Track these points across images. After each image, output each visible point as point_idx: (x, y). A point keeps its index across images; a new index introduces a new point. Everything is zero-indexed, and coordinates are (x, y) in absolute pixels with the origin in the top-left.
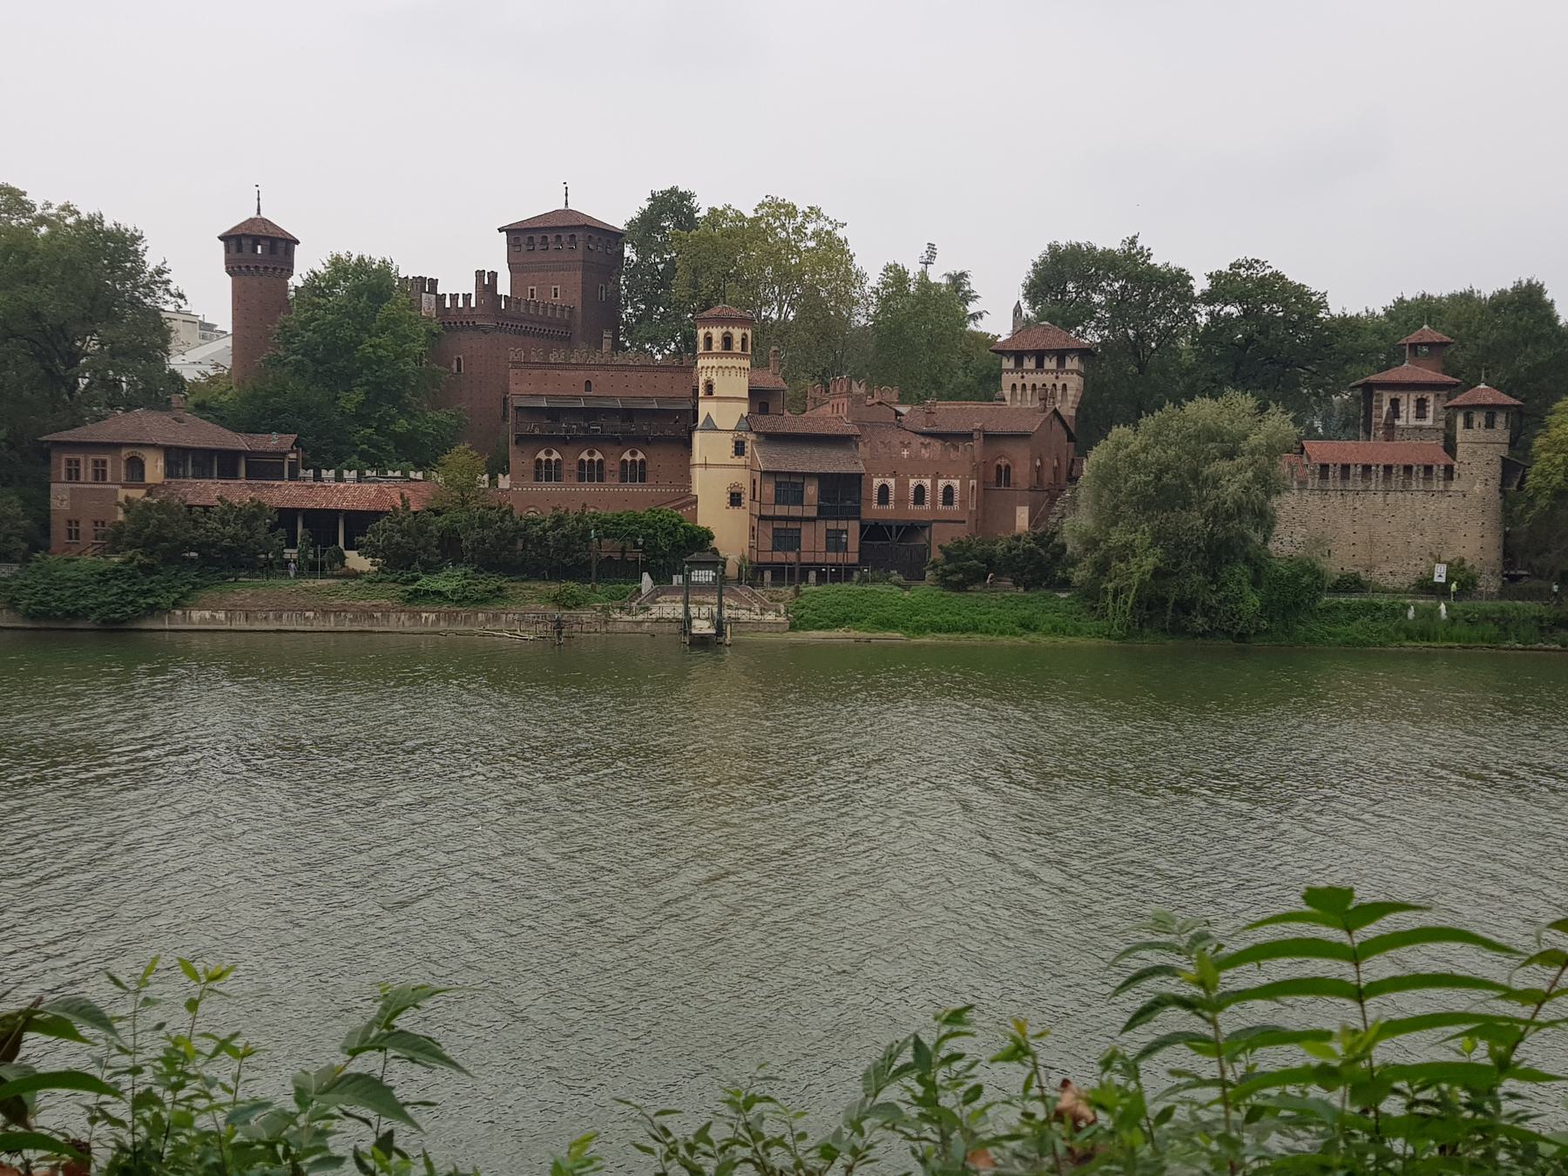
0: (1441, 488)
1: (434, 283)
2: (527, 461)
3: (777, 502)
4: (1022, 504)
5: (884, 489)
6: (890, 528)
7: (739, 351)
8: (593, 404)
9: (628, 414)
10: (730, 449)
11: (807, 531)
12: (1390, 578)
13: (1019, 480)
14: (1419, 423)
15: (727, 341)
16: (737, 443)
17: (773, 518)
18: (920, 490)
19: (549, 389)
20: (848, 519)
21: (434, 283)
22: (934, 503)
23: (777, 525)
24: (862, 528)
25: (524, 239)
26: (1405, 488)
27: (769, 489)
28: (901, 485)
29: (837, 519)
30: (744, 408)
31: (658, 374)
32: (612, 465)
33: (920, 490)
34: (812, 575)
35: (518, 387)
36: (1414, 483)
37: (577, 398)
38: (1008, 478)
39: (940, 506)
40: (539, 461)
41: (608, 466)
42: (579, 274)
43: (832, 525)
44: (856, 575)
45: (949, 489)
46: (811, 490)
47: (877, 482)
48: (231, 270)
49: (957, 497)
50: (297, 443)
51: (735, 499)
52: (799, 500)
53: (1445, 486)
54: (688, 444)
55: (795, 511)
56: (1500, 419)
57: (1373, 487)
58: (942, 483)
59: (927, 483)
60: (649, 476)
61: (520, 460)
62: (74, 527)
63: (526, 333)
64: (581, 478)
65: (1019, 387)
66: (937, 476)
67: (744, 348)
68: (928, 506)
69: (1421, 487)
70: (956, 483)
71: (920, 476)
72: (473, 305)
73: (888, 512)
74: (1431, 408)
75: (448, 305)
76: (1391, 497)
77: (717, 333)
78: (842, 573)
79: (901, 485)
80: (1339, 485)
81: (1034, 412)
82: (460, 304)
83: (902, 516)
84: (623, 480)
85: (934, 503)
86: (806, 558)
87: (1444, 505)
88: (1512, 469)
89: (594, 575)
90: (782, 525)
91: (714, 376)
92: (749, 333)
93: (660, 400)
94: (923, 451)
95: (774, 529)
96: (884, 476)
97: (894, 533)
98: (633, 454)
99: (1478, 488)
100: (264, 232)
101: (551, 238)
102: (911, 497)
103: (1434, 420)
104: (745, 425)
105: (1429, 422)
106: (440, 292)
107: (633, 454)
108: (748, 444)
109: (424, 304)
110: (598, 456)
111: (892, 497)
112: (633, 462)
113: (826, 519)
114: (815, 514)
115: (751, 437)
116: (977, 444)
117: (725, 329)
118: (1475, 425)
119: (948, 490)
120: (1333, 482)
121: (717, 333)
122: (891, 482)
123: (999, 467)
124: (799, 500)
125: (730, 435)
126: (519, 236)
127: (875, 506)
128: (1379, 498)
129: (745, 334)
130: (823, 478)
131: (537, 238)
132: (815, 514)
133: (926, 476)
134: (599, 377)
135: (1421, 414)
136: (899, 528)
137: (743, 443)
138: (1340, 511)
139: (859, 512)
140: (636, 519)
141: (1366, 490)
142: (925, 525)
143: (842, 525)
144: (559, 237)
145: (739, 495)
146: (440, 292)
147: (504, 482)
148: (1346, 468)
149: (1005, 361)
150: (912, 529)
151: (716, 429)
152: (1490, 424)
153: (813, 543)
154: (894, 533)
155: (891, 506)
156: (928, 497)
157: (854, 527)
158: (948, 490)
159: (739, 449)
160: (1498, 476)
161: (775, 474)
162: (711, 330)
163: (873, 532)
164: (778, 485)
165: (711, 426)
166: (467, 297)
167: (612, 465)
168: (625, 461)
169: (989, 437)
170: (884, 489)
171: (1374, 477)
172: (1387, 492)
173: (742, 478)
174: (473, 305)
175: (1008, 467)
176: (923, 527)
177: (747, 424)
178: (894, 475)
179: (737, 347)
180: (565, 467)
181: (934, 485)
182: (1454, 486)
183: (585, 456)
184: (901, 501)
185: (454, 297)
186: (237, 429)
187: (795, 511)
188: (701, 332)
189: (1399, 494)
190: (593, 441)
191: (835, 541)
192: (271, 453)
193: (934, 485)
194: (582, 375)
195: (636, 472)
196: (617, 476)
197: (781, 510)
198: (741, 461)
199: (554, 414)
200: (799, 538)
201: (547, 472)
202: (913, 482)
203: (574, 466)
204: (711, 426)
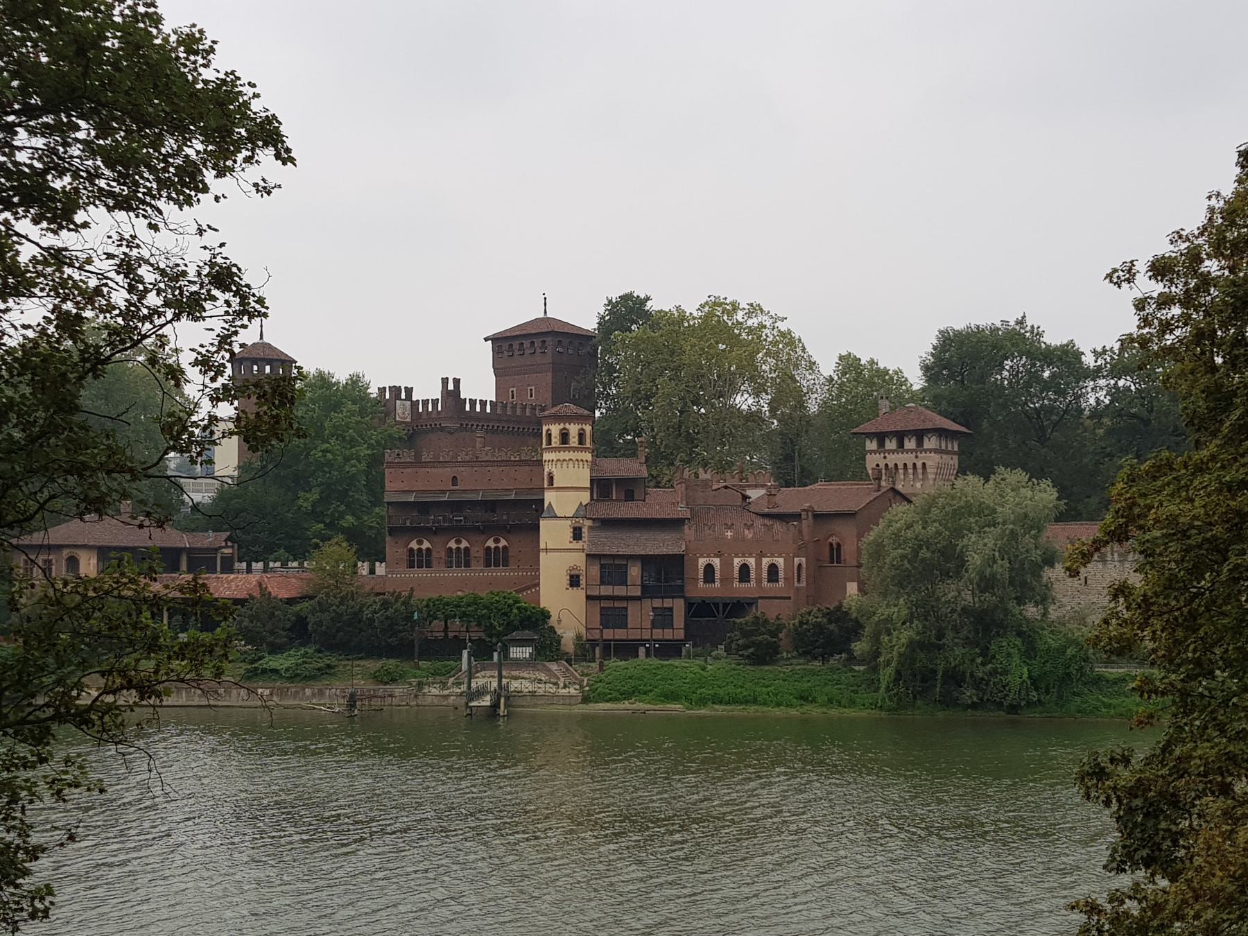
2: (400, 551)
3: (602, 583)
5: (709, 569)
6: (716, 605)
7: (576, 445)
8: (457, 498)
9: (491, 506)
10: (569, 534)
11: (633, 610)
13: (847, 557)
15: (564, 436)
16: (575, 529)
17: (600, 598)
18: (744, 569)
20: (673, 597)
21: (409, 391)
22: (759, 581)
23: (605, 604)
24: (689, 605)
25: (505, 346)
27: (595, 571)
28: (727, 565)
29: (662, 598)
30: (585, 497)
31: (516, 468)
32: (477, 552)
33: (744, 569)
34: (642, 650)
35: (392, 485)
37: (444, 492)
39: (765, 583)
40: (411, 550)
41: (473, 553)
42: (550, 374)
43: (657, 603)
46: (635, 571)
47: (702, 562)
49: (781, 574)
51: (574, 581)
52: (624, 582)
55: (620, 591)
58: (766, 562)
59: (752, 562)
60: (511, 560)
61: (393, 548)
66: (761, 555)
68: (753, 583)
70: (780, 562)
71: (744, 556)
72: (440, 409)
73: (715, 589)
75: (468, 408)
77: (555, 429)
78: (669, 649)
79: (727, 565)
84: (488, 565)
85: (759, 581)
86: (634, 635)
89: (416, 655)
90: (608, 604)
91: (554, 469)
93: (519, 491)
94: (746, 532)
95: (601, 608)
96: (709, 556)
97: (721, 608)
98: (497, 541)
100: (275, 357)
102: (736, 575)
107: (497, 541)
108: (585, 530)
109: (399, 411)
111: (717, 576)
112: (497, 548)
113: (652, 598)
114: (639, 594)
115: (588, 523)
116: (807, 524)
119: (773, 569)
121: (555, 429)
122: (716, 562)
123: (831, 544)
124: (624, 582)
125: (569, 522)
129: (582, 429)
130: (646, 560)
131: (516, 345)
132: (639, 594)
133: (751, 556)
134: (462, 473)
136: (725, 605)
137: (580, 529)
139: (683, 591)
140: (475, 601)
142: (752, 603)
143: (668, 603)
145: (578, 576)
147: (380, 569)
149: (868, 442)
150: (738, 607)
153: (640, 620)
154: (721, 608)
155: (717, 584)
156: (753, 575)
157: (679, 606)
158: (773, 569)
159: (577, 534)
161: (600, 557)
162: (551, 427)
163: (699, 610)
166: (435, 402)
167: (477, 552)
168: (489, 548)
169: (818, 517)
170: (709, 569)
173: (579, 560)
174: (440, 409)
175: (839, 545)
176: (750, 605)
177: (583, 512)
178: (716, 556)
179: (574, 441)
180: (434, 554)
181: (759, 564)
183: (452, 544)
184: (726, 579)
185: (425, 402)
187: (620, 591)
188: (545, 428)
190: (458, 531)
191: (663, 618)
192: (207, 549)
193: (759, 564)
194: (449, 472)
197: (607, 590)
199: (423, 508)
200: (626, 616)
201: (418, 560)
202: (737, 562)
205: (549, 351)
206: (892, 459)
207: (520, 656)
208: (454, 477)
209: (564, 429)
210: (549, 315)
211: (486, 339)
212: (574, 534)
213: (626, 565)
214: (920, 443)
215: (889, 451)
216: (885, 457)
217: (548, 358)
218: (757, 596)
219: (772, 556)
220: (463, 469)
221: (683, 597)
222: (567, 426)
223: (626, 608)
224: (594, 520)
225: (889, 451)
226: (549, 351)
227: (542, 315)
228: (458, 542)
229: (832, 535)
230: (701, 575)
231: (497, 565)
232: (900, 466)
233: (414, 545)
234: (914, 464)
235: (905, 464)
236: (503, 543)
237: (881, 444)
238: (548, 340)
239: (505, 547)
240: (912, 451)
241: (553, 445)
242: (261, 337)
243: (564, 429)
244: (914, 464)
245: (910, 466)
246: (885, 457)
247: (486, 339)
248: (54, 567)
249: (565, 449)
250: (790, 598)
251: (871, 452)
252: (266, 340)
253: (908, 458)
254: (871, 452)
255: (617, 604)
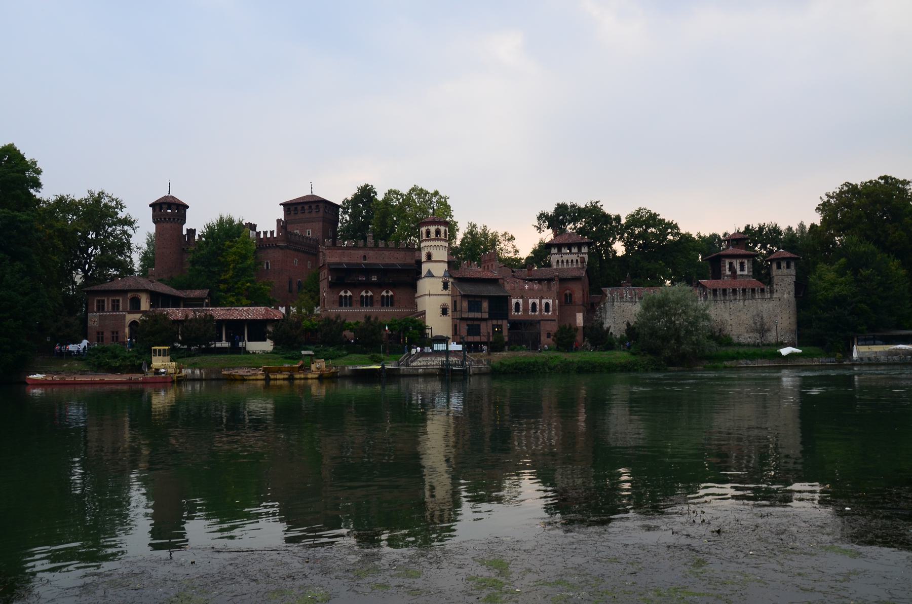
0: (769, 297)
1: (255, 226)
2: (335, 296)
4: (579, 312)
5: (517, 304)
10: (441, 286)
12: (749, 340)
14: (741, 273)
18: (534, 304)
19: (345, 260)
21: (255, 226)
23: (469, 322)
26: (753, 298)
27: (465, 304)
33: (534, 304)
35: (331, 259)
36: (757, 296)
37: (359, 264)
38: (571, 300)
39: (544, 313)
40: (341, 296)
41: (375, 298)
42: (321, 224)
43: (495, 322)
44: (506, 348)
45: (547, 304)
46: (485, 305)
48: (154, 222)
49: (551, 308)
50: (209, 294)
51: (444, 311)
52: (479, 310)
53: (771, 296)
54: (414, 287)
55: (478, 315)
56: (792, 264)
57: (738, 298)
58: (544, 301)
59: (537, 301)
62: (100, 335)
63: (298, 251)
64: (362, 305)
65: (560, 261)
66: (541, 298)
67: (446, 237)
68: (538, 313)
69: (760, 297)
70: (550, 301)
71: (534, 298)
72: (275, 235)
74: (746, 266)
76: (747, 302)
80: (722, 298)
81: (579, 269)
82: (269, 236)
83: (526, 318)
84: (383, 305)
85: (541, 310)
87: (771, 305)
88: (801, 287)
92: (447, 229)
96: (517, 298)
98: (387, 292)
99: (786, 296)
101: (306, 207)
102: (530, 308)
103: (748, 272)
104: (447, 275)
105: (746, 272)
106: (257, 231)
108: (450, 284)
109: (251, 236)
110: (370, 294)
111: (521, 308)
114: (487, 317)
115: (451, 280)
117: (436, 227)
118: (782, 267)
119: (547, 304)
120: (720, 297)
121: (433, 229)
122: (521, 301)
123: (566, 295)
125: (441, 280)
126: (289, 207)
127: (514, 313)
128: (741, 303)
130: (491, 299)
132: (487, 317)
133: (536, 298)
135: (742, 269)
138: (724, 310)
141: (735, 299)
142: (539, 322)
144: (310, 207)
146: (257, 231)
148: (724, 291)
151: (433, 276)
152: (788, 267)
155: (521, 313)
156: (538, 308)
157: (506, 325)
158: (547, 304)
159: (445, 286)
160: (794, 290)
163: (515, 325)
164: (469, 302)
165: (430, 275)
166: (272, 233)
169: (562, 280)
170: (517, 304)
171: (738, 293)
172: (744, 300)
173: (447, 301)
175: (571, 295)
178: (520, 298)
179: (443, 236)
180: (354, 299)
181: (541, 303)
182: (775, 296)
183: (363, 293)
185: (265, 233)
186: (177, 289)
189: (750, 301)
190: (368, 285)
193: (541, 303)
194: (361, 253)
195: (388, 302)
196: (380, 303)
198: (447, 292)
202: (531, 301)
203: (359, 299)
204: (430, 275)
205: (322, 210)
206: (565, 257)
207: (441, 349)
208: (365, 257)
209: (438, 229)
210: (313, 194)
211: (280, 204)
212: (444, 285)
213: (481, 302)
214: (580, 250)
215: (564, 254)
216: (562, 257)
217: (321, 213)
218: (540, 319)
219: (547, 298)
220: (369, 252)
221: (507, 319)
222: (439, 227)
223: (479, 326)
224: (455, 278)
225: (564, 254)
226: (322, 210)
227: (310, 194)
228: (367, 292)
229: (567, 290)
230: (513, 308)
231: (387, 305)
232: (570, 261)
233: (342, 293)
234: (577, 260)
235: (572, 260)
236: (391, 293)
237: (560, 250)
238: (321, 205)
239: (392, 296)
240: (576, 253)
241: (424, 238)
242: (169, 193)
243: (438, 229)
244: (577, 260)
245: (575, 261)
246: (562, 257)
247: (280, 204)
248: (121, 305)
249: (438, 240)
250: (554, 320)
251: (554, 254)
252: (172, 194)
253: (574, 257)
254: (554, 254)
255: (476, 323)
